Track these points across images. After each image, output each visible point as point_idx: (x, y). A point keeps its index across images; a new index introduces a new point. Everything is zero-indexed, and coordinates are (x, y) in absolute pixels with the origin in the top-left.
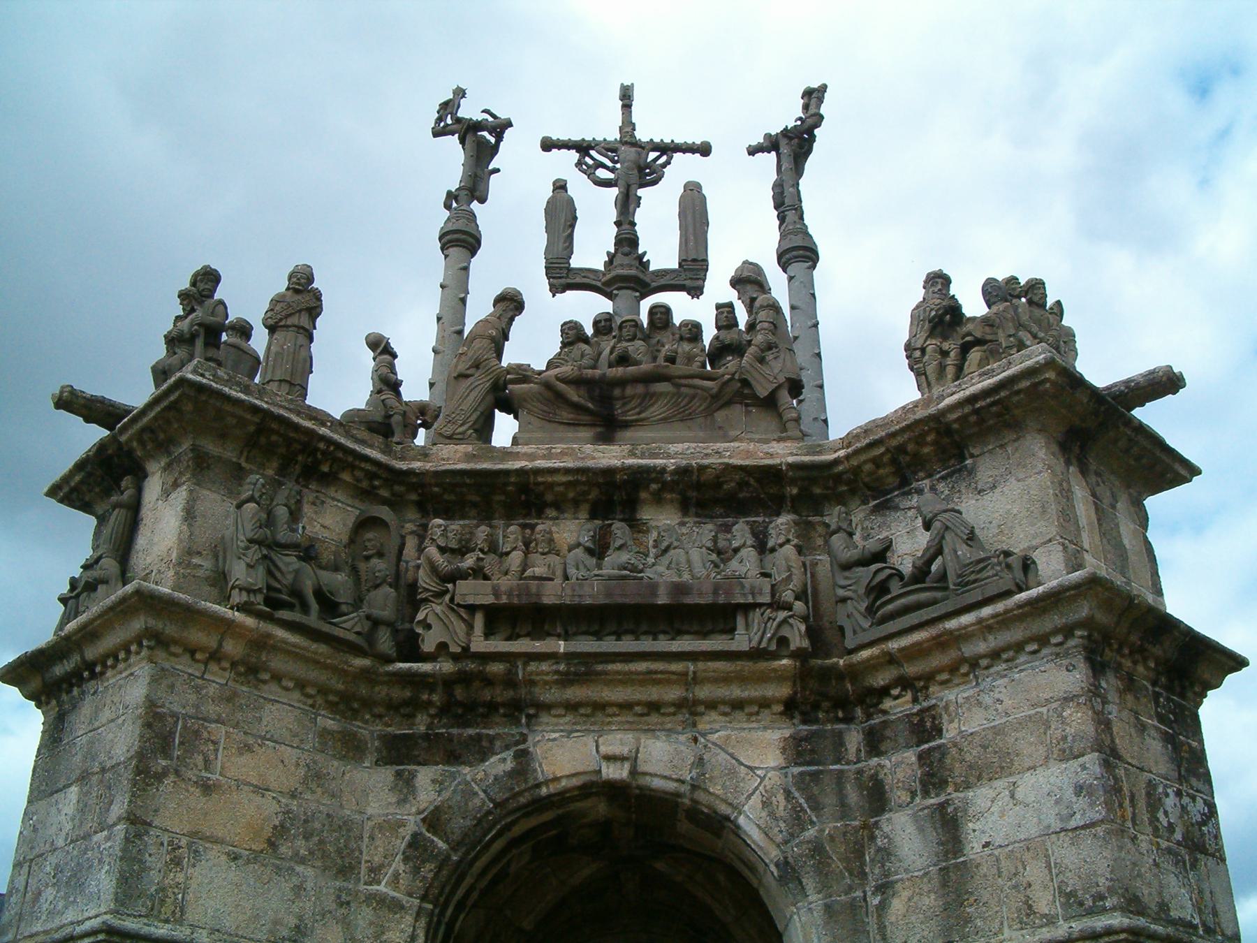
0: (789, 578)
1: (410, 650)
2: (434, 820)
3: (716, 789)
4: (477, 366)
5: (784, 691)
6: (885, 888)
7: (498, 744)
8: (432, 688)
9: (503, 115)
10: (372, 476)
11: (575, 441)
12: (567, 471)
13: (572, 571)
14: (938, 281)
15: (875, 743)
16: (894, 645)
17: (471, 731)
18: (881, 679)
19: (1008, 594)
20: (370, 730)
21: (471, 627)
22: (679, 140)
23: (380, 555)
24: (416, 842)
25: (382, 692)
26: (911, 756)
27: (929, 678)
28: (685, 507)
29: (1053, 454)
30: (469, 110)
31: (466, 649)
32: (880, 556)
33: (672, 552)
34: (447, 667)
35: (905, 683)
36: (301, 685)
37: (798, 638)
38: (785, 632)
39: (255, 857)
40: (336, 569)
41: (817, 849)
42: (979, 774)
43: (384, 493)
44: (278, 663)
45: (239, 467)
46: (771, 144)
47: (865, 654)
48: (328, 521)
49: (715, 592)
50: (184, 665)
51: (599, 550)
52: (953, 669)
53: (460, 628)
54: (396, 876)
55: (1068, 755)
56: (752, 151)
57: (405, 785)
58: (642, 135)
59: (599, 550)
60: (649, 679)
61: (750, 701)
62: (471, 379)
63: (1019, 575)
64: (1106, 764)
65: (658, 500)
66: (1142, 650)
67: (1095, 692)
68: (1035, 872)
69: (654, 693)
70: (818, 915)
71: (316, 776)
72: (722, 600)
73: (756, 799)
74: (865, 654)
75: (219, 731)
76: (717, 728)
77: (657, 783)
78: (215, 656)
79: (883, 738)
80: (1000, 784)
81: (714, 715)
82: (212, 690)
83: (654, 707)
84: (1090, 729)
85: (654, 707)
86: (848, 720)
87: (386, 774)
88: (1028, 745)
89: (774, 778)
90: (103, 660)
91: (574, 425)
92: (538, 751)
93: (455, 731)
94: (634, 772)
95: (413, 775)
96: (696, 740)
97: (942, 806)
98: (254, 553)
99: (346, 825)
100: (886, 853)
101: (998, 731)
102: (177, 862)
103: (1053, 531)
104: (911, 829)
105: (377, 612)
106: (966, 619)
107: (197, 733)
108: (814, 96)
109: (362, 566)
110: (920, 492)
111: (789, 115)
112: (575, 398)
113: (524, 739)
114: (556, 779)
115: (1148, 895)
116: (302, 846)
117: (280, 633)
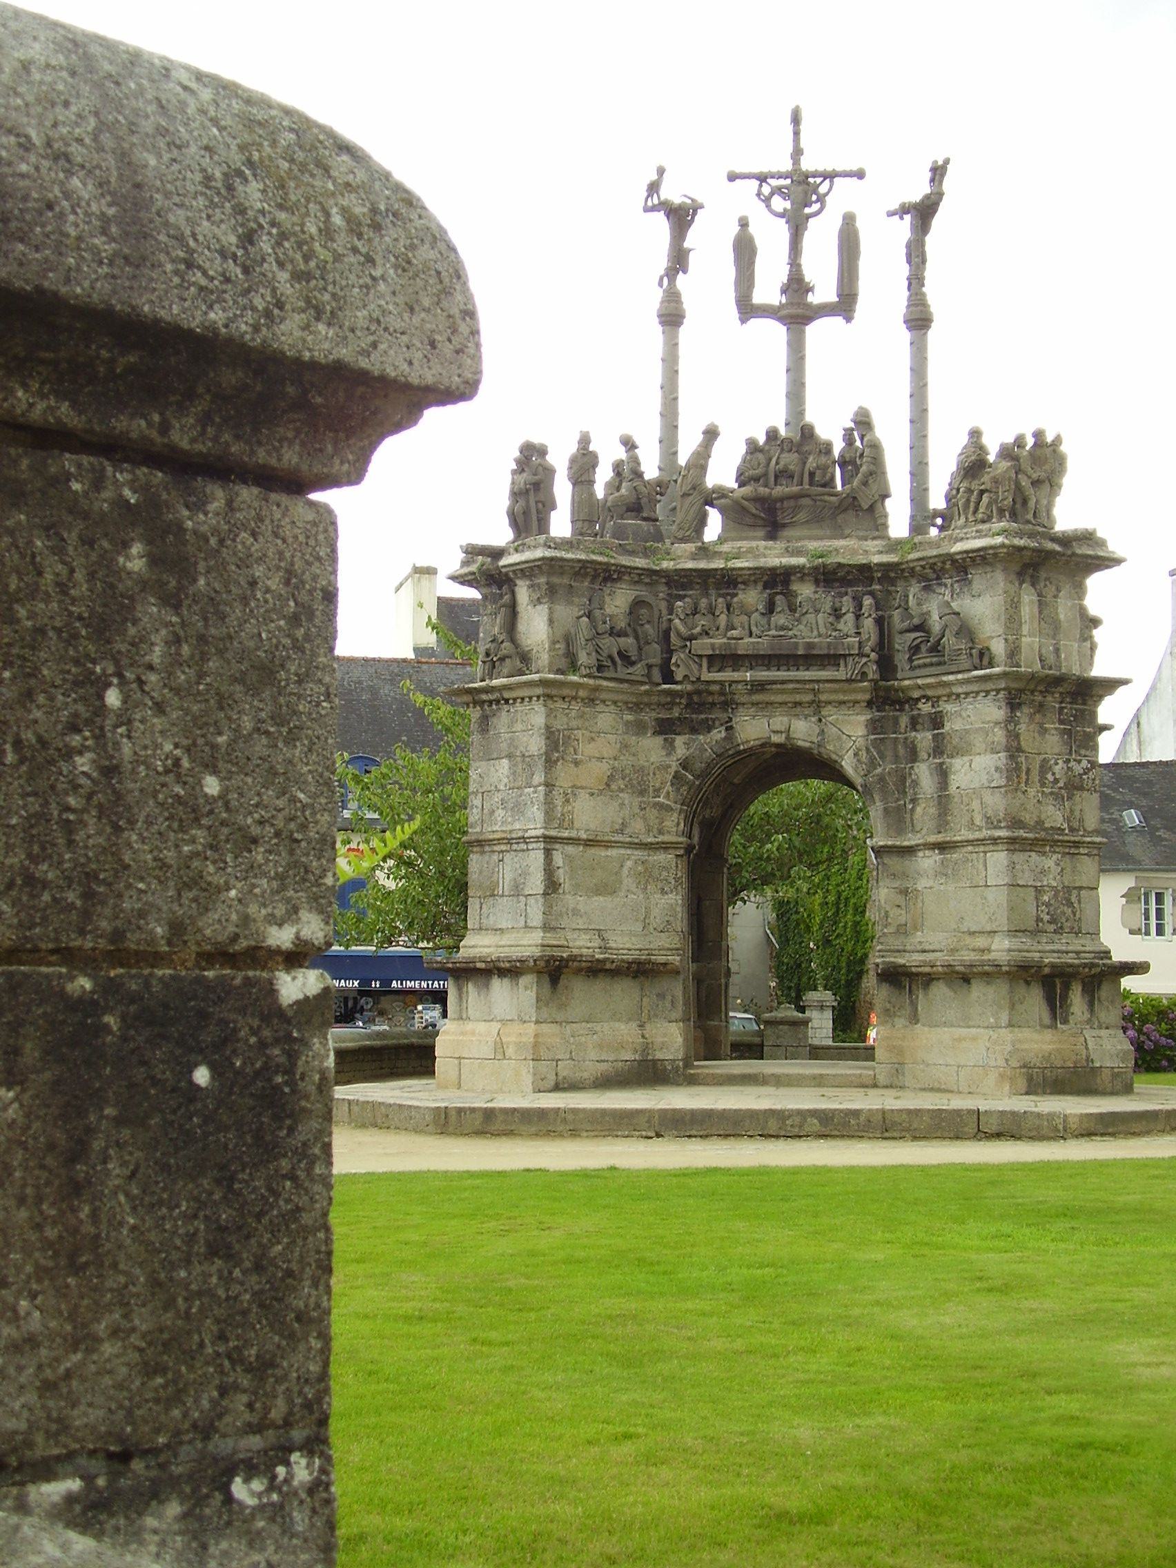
0: (869, 639)
1: (668, 677)
2: (685, 764)
3: (831, 747)
4: (694, 488)
5: (867, 697)
6: (914, 801)
7: (717, 723)
8: (681, 697)
9: (700, 200)
10: (640, 575)
11: (754, 538)
12: (749, 569)
13: (754, 629)
14: (975, 434)
15: (914, 724)
16: (920, 682)
17: (703, 716)
18: (916, 694)
19: (970, 671)
20: (649, 717)
21: (701, 666)
22: (839, 169)
23: (648, 622)
24: (677, 776)
25: (655, 699)
26: (929, 735)
27: (939, 697)
28: (817, 582)
29: (1011, 582)
30: (672, 193)
31: (699, 679)
32: (917, 628)
33: (808, 616)
34: (689, 687)
35: (928, 698)
36: (615, 703)
37: (872, 671)
38: (865, 670)
39: (601, 792)
40: (626, 635)
41: (881, 779)
42: (958, 752)
43: (647, 580)
44: (603, 696)
45: (571, 586)
46: (904, 210)
47: (907, 683)
48: (617, 604)
49: (829, 647)
50: (560, 704)
51: (770, 609)
52: (949, 696)
53: (694, 667)
54: (668, 793)
55: (994, 751)
56: (891, 214)
57: (670, 747)
58: (807, 164)
59: (770, 609)
60: (795, 691)
61: (849, 701)
62: (691, 498)
63: (976, 661)
64: (1012, 757)
65: (802, 579)
66: (1047, 691)
67: (1011, 720)
68: (975, 805)
69: (798, 698)
70: (880, 813)
71: (625, 746)
72: (832, 652)
73: (851, 753)
74: (907, 683)
75: (579, 734)
76: (832, 715)
77: (800, 743)
78: (575, 698)
79: (917, 723)
80: (966, 759)
81: (830, 707)
82: (573, 713)
83: (797, 704)
84: (1004, 741)
85: (797, 704)
86: (901, 710)
87: (659, 740)
88: (978, 742)
89: (861, 742)
90: (515, 700)
91: (754, 526)
92: (737, 727)
93: (694, 716)
94: (788, 738)
95: (674, 740)
96: (820, 720)
97: (941, 764)
98: (590, 647)
99: (642, 768)
100: (915, 783)
101: (967, 731)
102: (568, 801)
103: (1001, 631)
104: (927, 773)
105: (652, 661)
106: (951, 678)
107: (569, 737)
108: (938, 172)
109: (639, 629)
110: (946, 586)
111: (918, 190)
112: (754, 511)
113: (731, 719)
114: (748, 742)
115: (1028, 818)
116: (621, 784)
117: (605, 683)
